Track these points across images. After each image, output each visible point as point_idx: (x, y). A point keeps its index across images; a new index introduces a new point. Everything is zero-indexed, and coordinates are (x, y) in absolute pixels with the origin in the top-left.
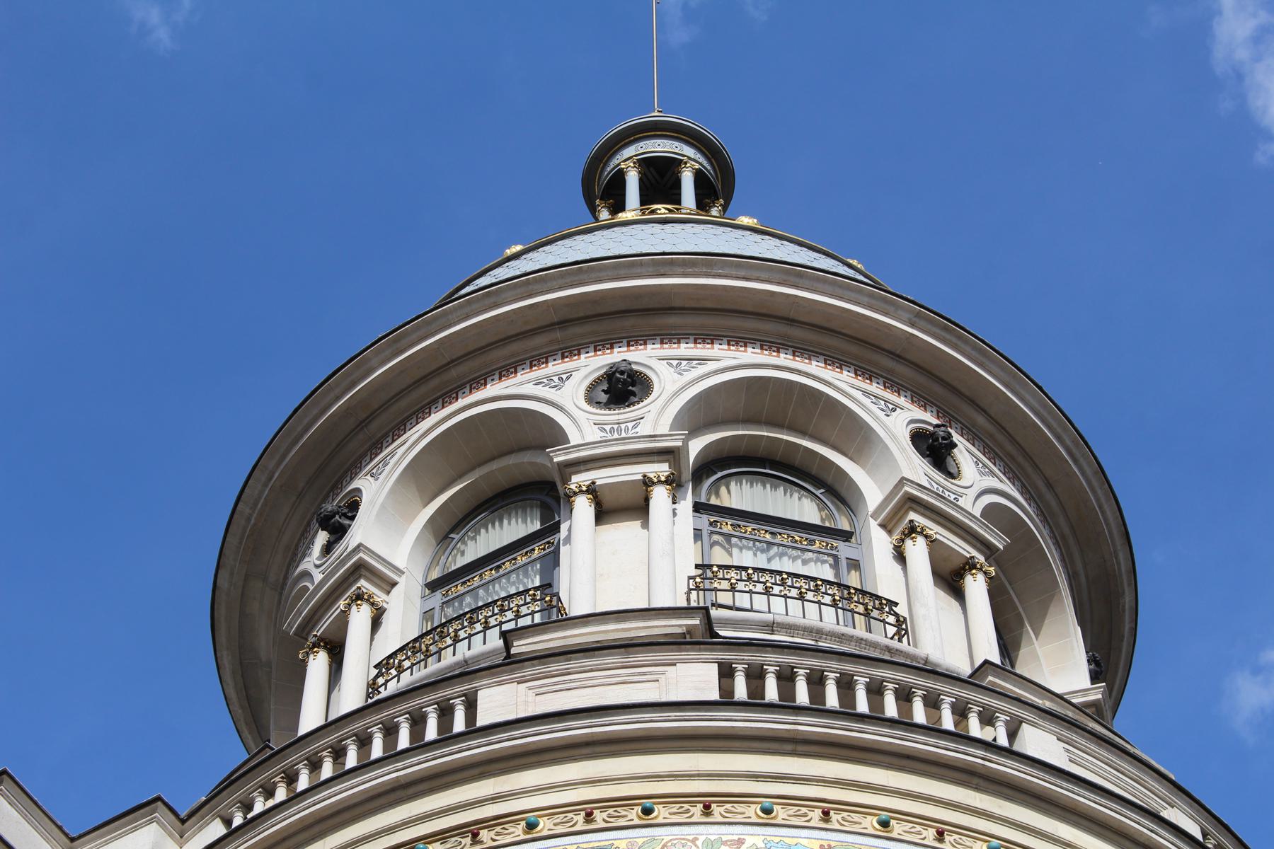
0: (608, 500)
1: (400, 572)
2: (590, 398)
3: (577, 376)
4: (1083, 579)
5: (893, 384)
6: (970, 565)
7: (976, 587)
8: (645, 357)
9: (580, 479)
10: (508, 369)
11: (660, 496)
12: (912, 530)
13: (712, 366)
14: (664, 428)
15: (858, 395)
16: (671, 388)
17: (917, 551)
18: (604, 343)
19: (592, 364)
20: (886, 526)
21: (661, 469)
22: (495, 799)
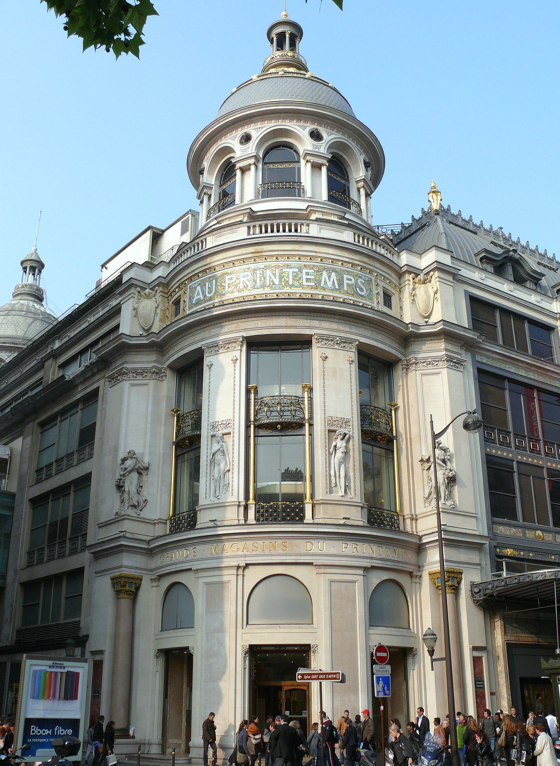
0: (244, 169)
1: (213, 185)
2: (241, 143)
3: (238, 136)
4: (365, 144)
5: (306, 121)
7: (324, 170)
11: (253, 168)
12: (307, 161)
13: (264, 129)
14: (253, 151)
15: (297, 127)
17: (309, 165)
19: (240, 132)
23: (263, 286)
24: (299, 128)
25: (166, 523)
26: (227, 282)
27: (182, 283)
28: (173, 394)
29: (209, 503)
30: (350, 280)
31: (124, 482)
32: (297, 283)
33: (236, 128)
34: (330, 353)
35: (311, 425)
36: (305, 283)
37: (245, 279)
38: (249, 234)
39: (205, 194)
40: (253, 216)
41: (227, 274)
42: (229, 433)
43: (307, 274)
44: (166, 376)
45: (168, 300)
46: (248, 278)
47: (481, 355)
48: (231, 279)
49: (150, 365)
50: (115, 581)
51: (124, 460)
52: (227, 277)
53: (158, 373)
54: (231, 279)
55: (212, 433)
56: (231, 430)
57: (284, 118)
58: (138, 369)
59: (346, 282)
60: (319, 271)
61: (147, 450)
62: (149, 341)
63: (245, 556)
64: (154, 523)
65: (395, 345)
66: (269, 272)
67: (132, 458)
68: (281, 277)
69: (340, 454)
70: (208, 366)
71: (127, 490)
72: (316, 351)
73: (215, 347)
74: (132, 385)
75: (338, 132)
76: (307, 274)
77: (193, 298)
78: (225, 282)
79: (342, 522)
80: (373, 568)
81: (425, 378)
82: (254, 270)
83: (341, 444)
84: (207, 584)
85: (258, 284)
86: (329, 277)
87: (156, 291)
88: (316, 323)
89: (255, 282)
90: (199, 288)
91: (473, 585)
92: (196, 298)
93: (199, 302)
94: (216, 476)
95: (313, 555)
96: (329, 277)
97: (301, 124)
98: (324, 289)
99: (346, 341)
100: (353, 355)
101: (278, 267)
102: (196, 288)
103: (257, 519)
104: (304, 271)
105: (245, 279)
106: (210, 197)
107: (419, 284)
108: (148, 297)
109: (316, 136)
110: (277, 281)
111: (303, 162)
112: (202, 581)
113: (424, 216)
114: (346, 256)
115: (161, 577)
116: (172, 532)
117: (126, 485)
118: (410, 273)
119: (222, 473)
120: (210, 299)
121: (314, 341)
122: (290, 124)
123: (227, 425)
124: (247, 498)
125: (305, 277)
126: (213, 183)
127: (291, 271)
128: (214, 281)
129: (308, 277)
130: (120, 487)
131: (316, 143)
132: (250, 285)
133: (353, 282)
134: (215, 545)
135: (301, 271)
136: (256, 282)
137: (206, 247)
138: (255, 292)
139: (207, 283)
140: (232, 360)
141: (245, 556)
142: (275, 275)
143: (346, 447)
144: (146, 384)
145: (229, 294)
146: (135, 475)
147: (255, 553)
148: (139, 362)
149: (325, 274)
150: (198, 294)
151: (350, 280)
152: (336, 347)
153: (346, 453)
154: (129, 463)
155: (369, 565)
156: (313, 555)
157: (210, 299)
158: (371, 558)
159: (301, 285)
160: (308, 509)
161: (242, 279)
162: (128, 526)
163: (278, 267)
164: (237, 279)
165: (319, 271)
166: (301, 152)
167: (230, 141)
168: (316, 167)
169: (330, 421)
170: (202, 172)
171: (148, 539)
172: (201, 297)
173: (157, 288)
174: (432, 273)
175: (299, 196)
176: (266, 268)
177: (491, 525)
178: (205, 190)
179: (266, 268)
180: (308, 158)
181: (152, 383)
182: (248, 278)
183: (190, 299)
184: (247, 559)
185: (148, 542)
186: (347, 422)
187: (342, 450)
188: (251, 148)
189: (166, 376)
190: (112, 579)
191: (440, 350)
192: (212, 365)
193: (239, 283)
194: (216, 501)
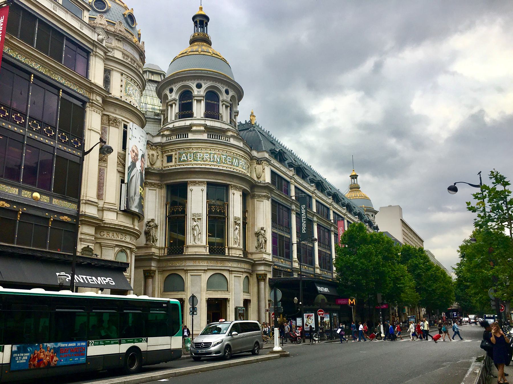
5: (224, 84)
6: (228, 106)
7: (229, 108)
8: (202, 82)
9: (195, 98)
10: (188, 80)
11: (202, 101)
12: (224, 104)
13: (208, 84)
15: (220, 86)
16: (204, 87)
17: (224, 106)
18: (198, 79)
20: (222, 102)
21: (202, 98)
22: (190, 146)
23: (213, 161)
24: (221, 87)
25: (164, 249)
26: (199, 156)
27: (174, 149)
28: (165, 195)
29: (192, 245)
30: (241, 162)
31: (150, 232)
32: (225, 162)
33: (194, 80)
34: (235, 192)
35: (227, 218)
36: (228, 163)
37: (207, 157)
38: (208, 137)
39: (174, 103)
40: (209, 130)
41: (198, 152)
42: (200, 219)
43: (229, 159)
44: (163, 187)
45: (162, 153)
46: (208, 156)
47: (273, 194)
48: (200, 155)
49: (158, 182)
50: (145, 272)
51: (149, 222)
52: (199, 154)
53: (160, 187)
54: (200, 155)
55: (193, 218)
56: (201, 218)
57: (216, 82)
58: (153, 183)
59: (240, 163)
60: (233, 158)
61: (156, 219)
62: (159, 172)
63: (208, 266)
64: (160, 249)
65: (250, 188)
66: (216, 156)
67: (153, 222)
68: (220, 159)
69: (237, 231)
70: (190, 190)
71: (152, 235)
72: (231, 191)
73: (195, 183)
74: (149, 190)
75: (235, 91)
76: (229, 159)
77: (181, 158)
78: (197, 156)
79: (238, 255)
80: (245, 272)
81: (257, 202)
82: (210, 154)
83: (238, 227)
84: (191, 275)
85: (212, 160)
86: (236, 161)
87: (157, 148)
88: (231, 180)
89: (210, 158)
90: (184, 154)
91: (269, 278)
92: (182, 159)
93: (184, 161)
94: (196, 235)
95: (230, 267)
96: (236, 161)
97: (222, 85)
98: (234, 166)
99: (241, 188)
100: (241, 193)
101: (219, 154)
102: (182, 154)
103: (209, 252)
104: (228, 157)
105: (207, 157)
106: (176, 105)
107: (258, 164)
108: (153, 149)
109: (227, 92)
110: (219, 161)
111: (221, 104)
112: (189, 274)
113: (246, 124)
114: (241, 153)
115: (164, 271)
116: (170, 253)
117: (151, 233)
118: (255, 159)
119: (198, 233)
120: (191, 161)
121: (230, 187)
122: (218, 84)
123: (199, 215)
124: (206, 244)
125: (228, 160)
126: (177, 98)
127: (224, 157)
128: (192, 154)
129: (229, 160)
130: (147, 234)
131: (227, 95)
132: (208, 160)
133: (242, 164)
134: (195, 261)
135: (227, 157)
136: (211, 159)
137: (188, 137)
138: (210, 163)
139: (189, 154)
140: (202, 190)
141: (208, 266)
142: (218, 157)
143: (239, 228)
144: (155, 190)
145: (199, 162)
146: (154, 229)
147: (210, 265)
148: (152, 180)
149: (234, 160)
150: (184, 157)
151: (241, 162)
152: (237, 190)
153: (239, 230)
154: (152, 224)
155: (244, 271)
156: (230, 267)
157: (191, 161)
158: (244, 268)
159: (227, 163)
160: (227, 250)
161: (205, 156)
162: (153, 250)
163: (219, 154)
164: (203, 156)
165: (233, 158)
166: (221, 99)
167: (190, 83)
168: (227, 107)
169: (236, 218)
170: (171, 91)
171: (158, 255)
172: (185, 158)
173: (158, 147)
174: (263, 161)
175: (219, 120)
176: (215, 154)
177: (273, 257)
178: (174, 101)
179: (215, 154)
180: (224, 103)
181: (157, 189)
182: (208, 156)
183: (179, 158)
184: (208, 267)
185: (159, 256)
186: (239, 219)
187: (238, 229)
188: (202, 92)
189: (163, 187)
190: (144, 271)
191: (264, 192)
192: (192, 190)
193: (204, 158)
194: (195, 244)
